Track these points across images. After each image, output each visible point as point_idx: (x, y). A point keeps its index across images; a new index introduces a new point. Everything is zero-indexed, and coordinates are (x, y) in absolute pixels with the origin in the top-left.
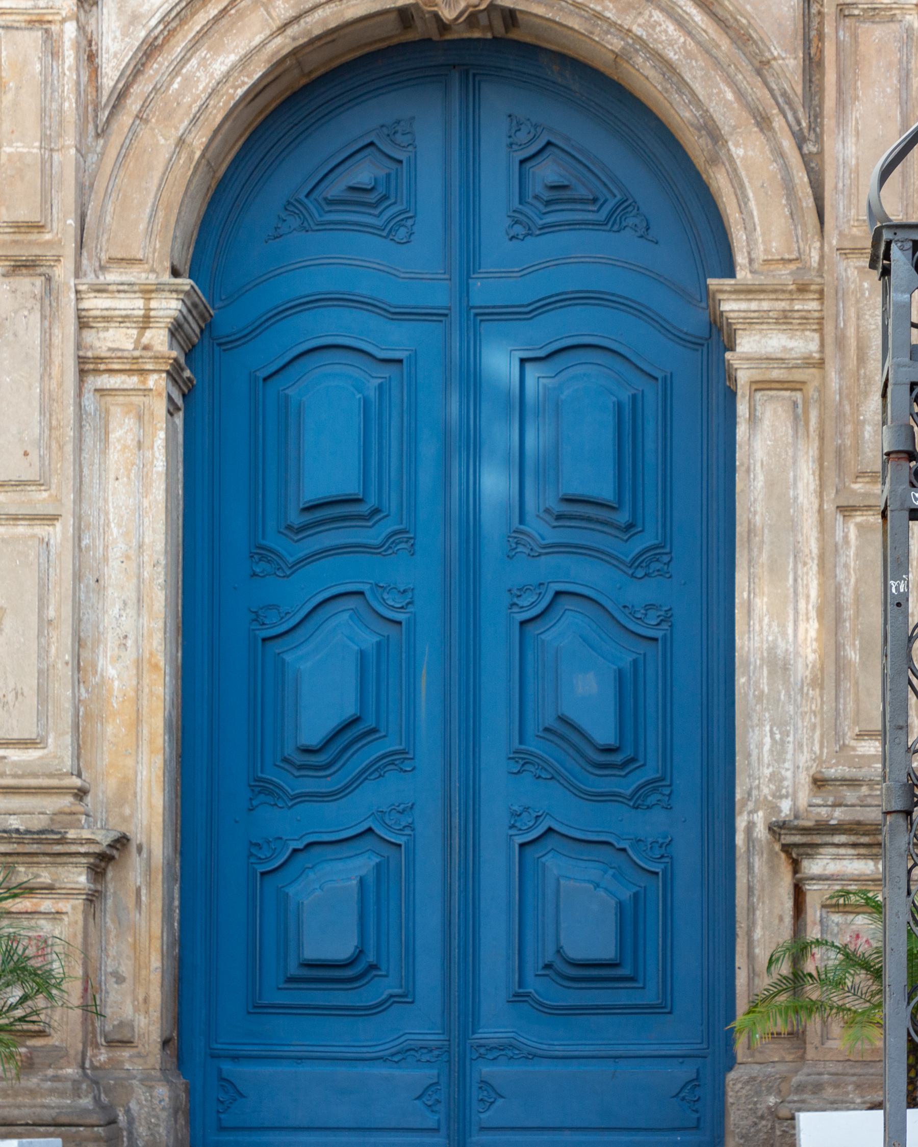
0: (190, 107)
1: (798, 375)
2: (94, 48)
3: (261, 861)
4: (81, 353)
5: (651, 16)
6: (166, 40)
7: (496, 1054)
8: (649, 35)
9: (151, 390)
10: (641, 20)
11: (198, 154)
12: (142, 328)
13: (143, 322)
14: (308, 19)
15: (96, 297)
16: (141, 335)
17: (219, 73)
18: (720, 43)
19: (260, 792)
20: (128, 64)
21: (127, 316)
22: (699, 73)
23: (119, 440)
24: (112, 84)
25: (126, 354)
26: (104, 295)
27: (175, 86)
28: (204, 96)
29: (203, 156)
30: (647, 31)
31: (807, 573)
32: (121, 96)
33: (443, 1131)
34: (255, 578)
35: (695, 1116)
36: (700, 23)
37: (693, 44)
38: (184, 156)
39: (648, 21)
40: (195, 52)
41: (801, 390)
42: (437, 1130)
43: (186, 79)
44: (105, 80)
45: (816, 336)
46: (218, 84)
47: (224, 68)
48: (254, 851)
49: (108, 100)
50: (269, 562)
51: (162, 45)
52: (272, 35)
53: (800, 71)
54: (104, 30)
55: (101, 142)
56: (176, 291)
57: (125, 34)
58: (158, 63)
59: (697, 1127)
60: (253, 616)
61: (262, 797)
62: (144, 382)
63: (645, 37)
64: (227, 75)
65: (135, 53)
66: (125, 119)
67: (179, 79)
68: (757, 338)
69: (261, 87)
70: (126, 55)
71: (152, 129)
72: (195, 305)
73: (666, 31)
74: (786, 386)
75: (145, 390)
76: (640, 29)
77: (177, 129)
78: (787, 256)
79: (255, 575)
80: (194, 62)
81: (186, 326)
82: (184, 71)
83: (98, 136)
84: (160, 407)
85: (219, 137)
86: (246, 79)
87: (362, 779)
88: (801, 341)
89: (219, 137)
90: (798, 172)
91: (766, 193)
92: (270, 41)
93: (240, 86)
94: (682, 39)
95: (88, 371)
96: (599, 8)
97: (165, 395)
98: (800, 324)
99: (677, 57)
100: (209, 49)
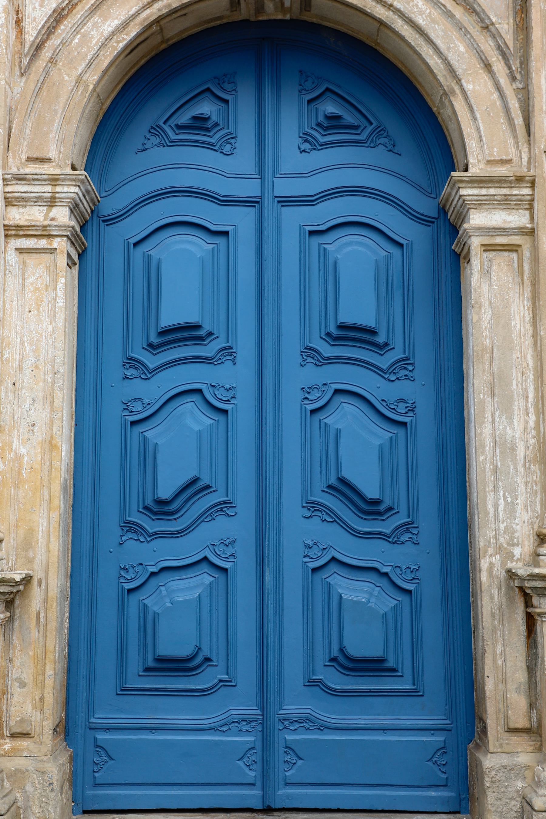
1: (516, 240)
2: (20, 16)
3: (129, 581)
4: (6, 223)
6: (70, 11)
7: (297, 725)
8: (405, 7)
9: (56, 249)
11: (91, 87)
12: (50, 206)
13: (51, 202)
15: (17, 184)
17: (107, 32)
18: (455, 13)
19: (127, 531)
20: (43, 26)
21: (39, 197)
22: (441, 33)
23: (32, 284)
24: (32, 39)
25: (38, 224)
26: (23, 182)
27: (76, 41)
28: (96, 48)
29: (94, 90)
30: (404, 5)
31: (526, 381)
32: (39, 47)
33: (259, 784)
34: (126, 380)
35: (445, 776)
37: (436, 14)
38: (81, 89)
40: (90, 19)
41: (517, 251)
42: (253, 784)
43: (84, 36)
44: (27, 36)
45: (527, 213)
46: (106, 40)
47: (110, 29)
48: (123, 573)
49: (29, 50)
50: (136, 368)
51: (67, 15)
52: (143, 7)
53: (511, 31)
54: (27, 3)
55: (24, 79)
56: (74, 180)
57: (41, 6)
58: (64, 25)
59: (445, 786)
60: (125, 406)
61: (130, 535)
62: (51, 244)
63: (402, 9)
64: (113, 34)
65: (48, 19)
66: (41, 63)
67: (79, 36)
68: (485, 214)
69: (135, 44)
70: (42, 20)
72: (88, 192)
73: (417, 5)
74: (506, 248)
75: (51, 249)
76: (399, 4)
77: (77, 70)
78: (504, 158)
79: (126, 378)
80: (89, 24)
81: (81, 206)
82: (82, 31)
83: (22, 75)
84: (63, 261)
85: (106, 78)
86: (125, 37)
87: (200, 521)
88: (516, 217)
89: (106, 78)
90: (511, 100)
91: (489, 114)
92: (142, 12)
93: (120, 41)
94: (428, 11)
95: (11, 236)
97: (66, 252)
98: (516, 204)
99: (425, 23)
100: (100, 17)
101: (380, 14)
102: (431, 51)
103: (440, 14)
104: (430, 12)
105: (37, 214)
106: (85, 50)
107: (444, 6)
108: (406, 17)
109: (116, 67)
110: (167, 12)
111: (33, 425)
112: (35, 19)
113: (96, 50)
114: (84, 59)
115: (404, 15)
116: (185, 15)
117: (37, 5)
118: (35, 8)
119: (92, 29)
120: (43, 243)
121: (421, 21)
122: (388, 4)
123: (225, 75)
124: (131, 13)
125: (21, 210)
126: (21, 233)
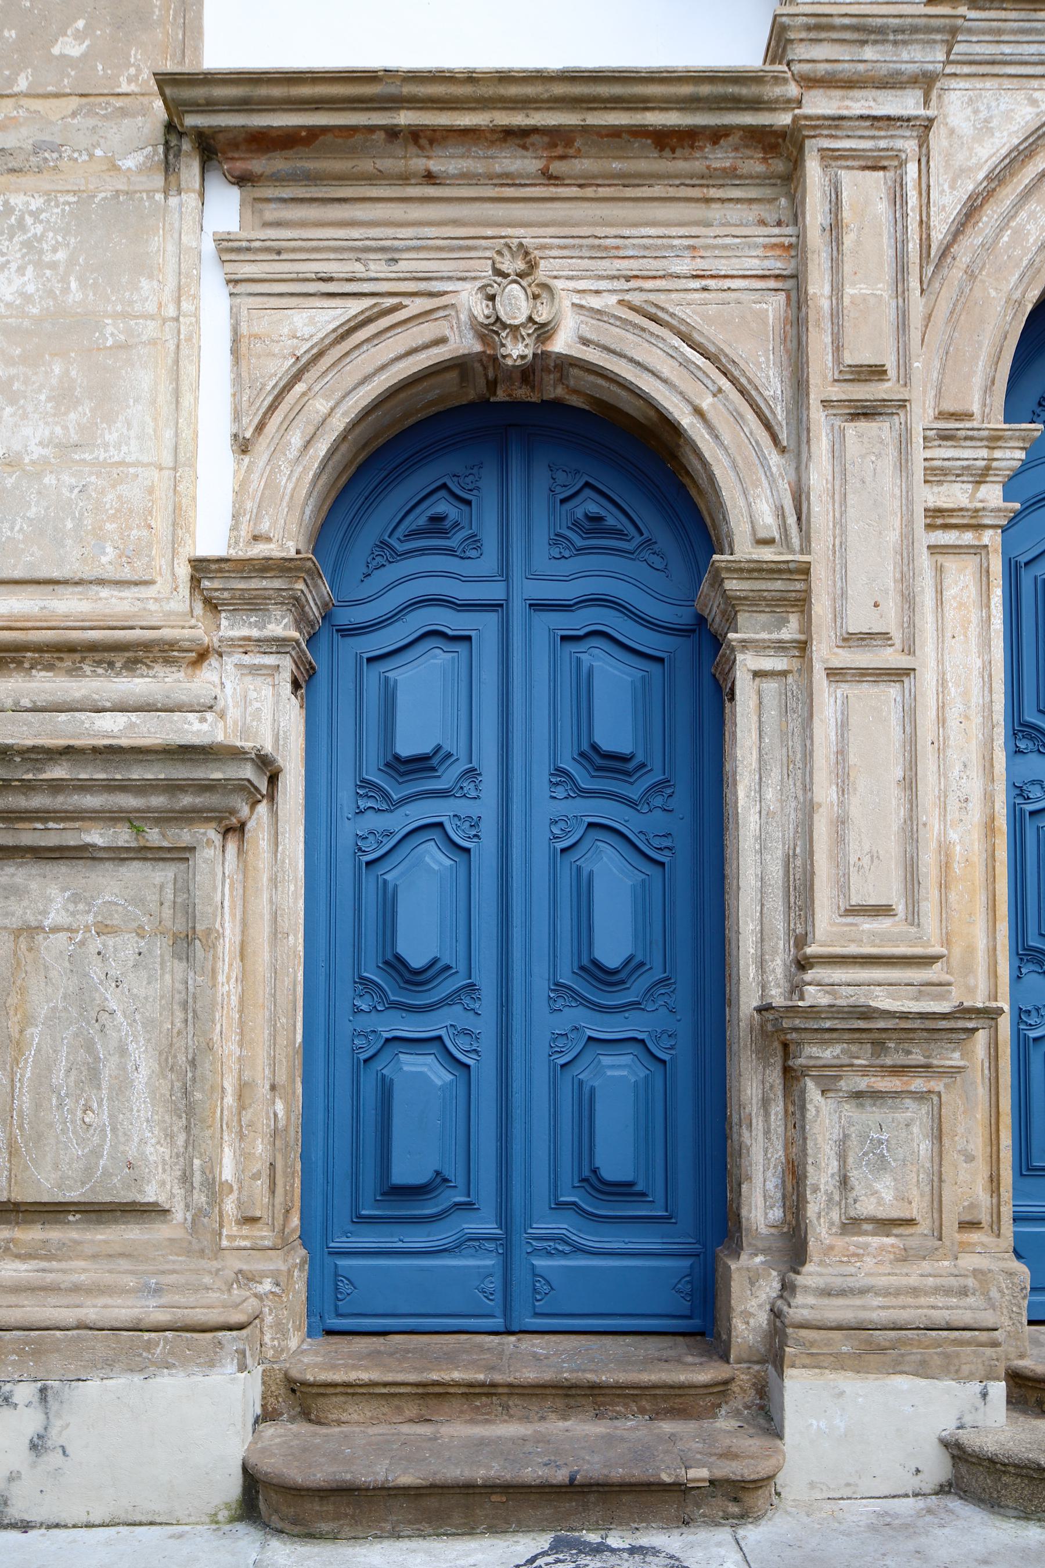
0: (1021, 259)
12: (977, 482)
13: (981, 475)
16: (976, 490)
23: (954, 598)
24: (941, 237)
27: (1005, 239)
28: (1034, 249)
43: (1016, 232)
57: (953, 187)
58: (987, 216)
67: (1009, 232)
71: (983, 282)
75: (978, 546)
77: (1008, 281)
80: (1023, 215)
100: (1038, 202)
105: (959, 495)
106: (1018, 252)
111: (966, 800)
112: (944, 207)
114: (1017, 265)
117: (946, 187)
118: (943, 191)
119: (1028, 222)
120: (968, 538)
125: (936, 489)
126: (939, 521)
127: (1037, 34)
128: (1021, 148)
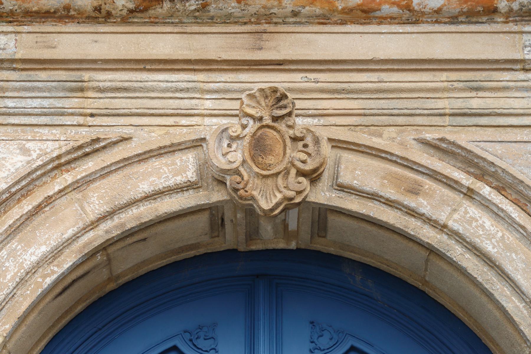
5: (466, 212)
10: (456, 216)
14: (123, 216)
17: (29, 263)
22: (521, 265)
28: (11, 285)
30: (463, 226)
36: (517, 219)
37: (511, 239)
39: (464, 217)
46: (27, 273)
47: (34, 259)
52: (84, 229)
63: (461, 232)
69: (69, 280)
73: (483, 226)
76: (456, 224)
85: (23, 328)
86: (56, 269)
92: (83, 235)
94: (500, 234)
96: (413, 205)
99: (496, 250)
101: (428, 238)
102: (507, 291)
103: (517, 238)
104: (503, 235)
107: (523, 227)
108: (467, 242)
109: (39, 313)
110: (118, 235)
113: (11, 288)
115: (464, 240)
116: (145, 239)
119: (7, 259)
121: (489, 248)
122: (439, 224)
123: (200, 328)
124: (66, 236)
127: (39, 92)
128: (13, 190)
